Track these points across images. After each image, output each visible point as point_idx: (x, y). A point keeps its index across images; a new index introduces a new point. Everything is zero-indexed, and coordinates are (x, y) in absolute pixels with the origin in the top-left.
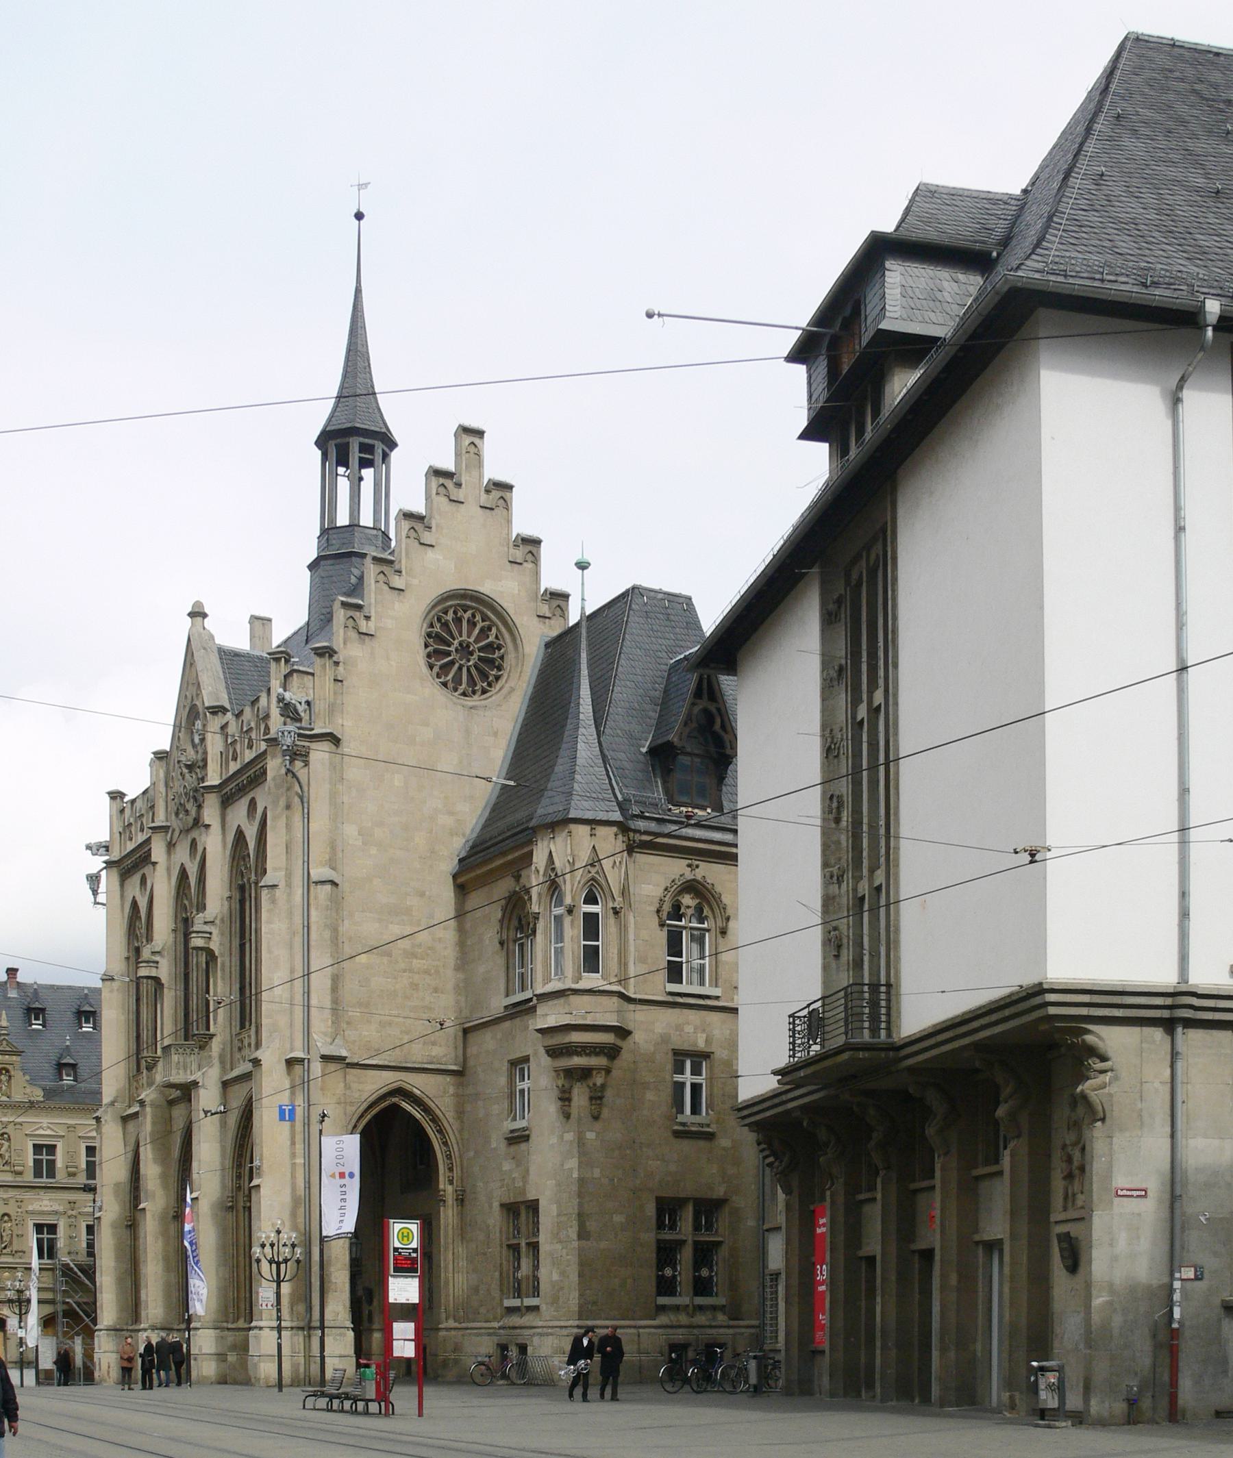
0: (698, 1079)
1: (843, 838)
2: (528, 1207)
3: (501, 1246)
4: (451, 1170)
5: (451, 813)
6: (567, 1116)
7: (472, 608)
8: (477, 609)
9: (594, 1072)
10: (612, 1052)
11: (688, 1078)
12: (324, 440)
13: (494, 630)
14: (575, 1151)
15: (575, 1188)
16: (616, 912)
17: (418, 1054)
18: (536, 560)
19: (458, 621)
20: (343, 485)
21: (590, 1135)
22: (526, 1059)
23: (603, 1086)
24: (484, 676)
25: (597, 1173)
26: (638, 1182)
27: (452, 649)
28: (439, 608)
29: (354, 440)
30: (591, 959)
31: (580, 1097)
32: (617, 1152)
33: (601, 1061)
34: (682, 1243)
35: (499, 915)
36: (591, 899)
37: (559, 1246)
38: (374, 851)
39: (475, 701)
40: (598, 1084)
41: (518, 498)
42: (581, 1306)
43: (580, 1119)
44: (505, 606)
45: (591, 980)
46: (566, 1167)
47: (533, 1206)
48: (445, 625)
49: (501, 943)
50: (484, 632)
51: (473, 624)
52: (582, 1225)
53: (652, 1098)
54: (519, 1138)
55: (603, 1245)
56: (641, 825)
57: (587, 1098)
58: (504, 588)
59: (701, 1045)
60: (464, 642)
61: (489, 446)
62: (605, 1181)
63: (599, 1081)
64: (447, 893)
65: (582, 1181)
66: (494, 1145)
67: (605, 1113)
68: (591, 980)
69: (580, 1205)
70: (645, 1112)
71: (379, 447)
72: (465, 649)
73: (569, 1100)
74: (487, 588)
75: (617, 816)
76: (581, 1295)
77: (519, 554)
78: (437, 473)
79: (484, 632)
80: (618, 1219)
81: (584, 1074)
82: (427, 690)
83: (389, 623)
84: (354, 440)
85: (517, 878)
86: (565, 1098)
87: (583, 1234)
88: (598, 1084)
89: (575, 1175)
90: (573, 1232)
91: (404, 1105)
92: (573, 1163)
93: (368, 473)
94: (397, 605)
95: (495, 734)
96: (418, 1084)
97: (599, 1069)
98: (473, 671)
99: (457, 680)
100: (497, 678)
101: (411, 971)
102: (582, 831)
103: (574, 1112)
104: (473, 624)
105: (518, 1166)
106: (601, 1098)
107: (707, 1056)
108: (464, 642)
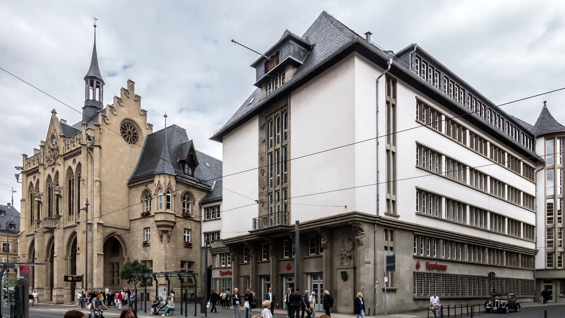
0: (189, 235)
1: (264, 179)
6: (162, 241)
10: (172, 227)
11: (186, 235)
12: (86, 78)
16: (174, 196)
17: (119, 225)
19: (128, 126)
20: (91, 91)
21: (167, 246)
22: (149, 228)
25: (168, 254)
29: (94, 80)
30: (168, 206)
31: (165, 237)
35: (141, 194)
36: (168, 192)
39: (132, 145)
45: (168, 211)
47: (151, 262)
48: (125, 126)
51: (131, 127)
56: (178, 177)
58: (139, 120)
59: (189, 228)
60: (129, 131)
63: (170, 233)
64: (126, 188)
65: (166, 256)
68: (168, 211)
71: (101, 84)
72: (129, 133)
74: (135, 119)
75: (175, 174)
77: (142, 113)
80: (173, 265)
81: (166, 232)
82: (121, 140)
84: (94, 80)
85: (146, 186)
86: (161, 237)
93: (98, 89)
99: (128, 139)
102: (167, 177)
104: (131, 127)
107: (190, 230)
108: (129, 131)
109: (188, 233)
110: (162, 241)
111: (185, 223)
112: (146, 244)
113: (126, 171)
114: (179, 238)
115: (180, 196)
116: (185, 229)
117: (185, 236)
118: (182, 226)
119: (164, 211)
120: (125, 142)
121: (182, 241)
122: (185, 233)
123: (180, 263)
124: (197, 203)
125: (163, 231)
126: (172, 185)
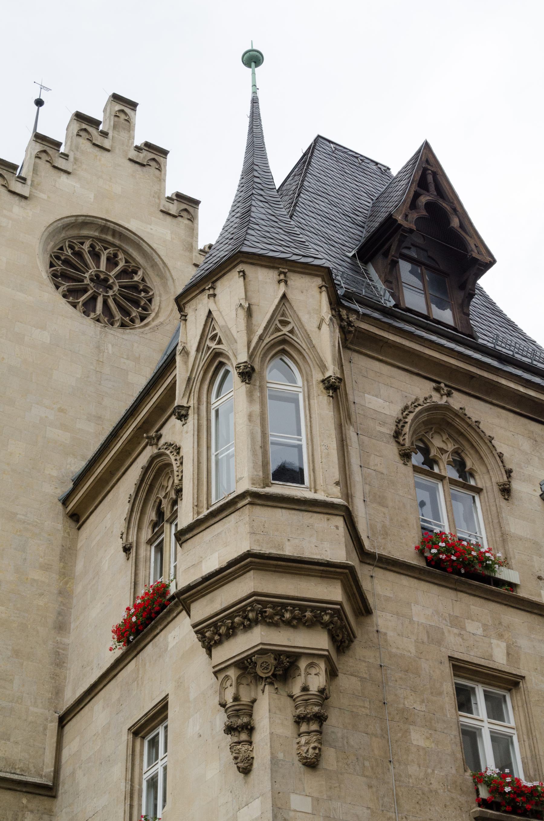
6: (246, 769)
8: (120, 248)
9: (303, 664)
10: (343, 640)
13: (140, 273)
18: (193, 219)
23: (323, 694)
24: (125, 312)
27: (87, 275)
28: (74, 232)
31: (271, 714)
33: (319, 641)
40: (314, 689)
41: (171, 163)
43: (274, 761)
44: (154, 246)
49: (127, 550)
50: (127, 273)
51: (112, 261)
53: (422, 743)
57: (290, 722)
61: (140, 118)
63: (317, 681)
67: (330, 758)
70: (413, 769)
73: (249, 729)
74: (133, 225)
77: (174, 208)
78: (79, 117)
86: (240, 725)
97: (314, 656)
100: (142, 319)
106: (320, 718)
109: (496, 711)
110: (246, 769)
111: (456, 622)
114: (418, 738)
115: (389, 430)
116: (459, 667)
117: (470, 736)
118: (434, 637)
120: (63, 305)
121: (449, 766)
122: (464, 702)
125: (245, 666)
126: (309, 322)
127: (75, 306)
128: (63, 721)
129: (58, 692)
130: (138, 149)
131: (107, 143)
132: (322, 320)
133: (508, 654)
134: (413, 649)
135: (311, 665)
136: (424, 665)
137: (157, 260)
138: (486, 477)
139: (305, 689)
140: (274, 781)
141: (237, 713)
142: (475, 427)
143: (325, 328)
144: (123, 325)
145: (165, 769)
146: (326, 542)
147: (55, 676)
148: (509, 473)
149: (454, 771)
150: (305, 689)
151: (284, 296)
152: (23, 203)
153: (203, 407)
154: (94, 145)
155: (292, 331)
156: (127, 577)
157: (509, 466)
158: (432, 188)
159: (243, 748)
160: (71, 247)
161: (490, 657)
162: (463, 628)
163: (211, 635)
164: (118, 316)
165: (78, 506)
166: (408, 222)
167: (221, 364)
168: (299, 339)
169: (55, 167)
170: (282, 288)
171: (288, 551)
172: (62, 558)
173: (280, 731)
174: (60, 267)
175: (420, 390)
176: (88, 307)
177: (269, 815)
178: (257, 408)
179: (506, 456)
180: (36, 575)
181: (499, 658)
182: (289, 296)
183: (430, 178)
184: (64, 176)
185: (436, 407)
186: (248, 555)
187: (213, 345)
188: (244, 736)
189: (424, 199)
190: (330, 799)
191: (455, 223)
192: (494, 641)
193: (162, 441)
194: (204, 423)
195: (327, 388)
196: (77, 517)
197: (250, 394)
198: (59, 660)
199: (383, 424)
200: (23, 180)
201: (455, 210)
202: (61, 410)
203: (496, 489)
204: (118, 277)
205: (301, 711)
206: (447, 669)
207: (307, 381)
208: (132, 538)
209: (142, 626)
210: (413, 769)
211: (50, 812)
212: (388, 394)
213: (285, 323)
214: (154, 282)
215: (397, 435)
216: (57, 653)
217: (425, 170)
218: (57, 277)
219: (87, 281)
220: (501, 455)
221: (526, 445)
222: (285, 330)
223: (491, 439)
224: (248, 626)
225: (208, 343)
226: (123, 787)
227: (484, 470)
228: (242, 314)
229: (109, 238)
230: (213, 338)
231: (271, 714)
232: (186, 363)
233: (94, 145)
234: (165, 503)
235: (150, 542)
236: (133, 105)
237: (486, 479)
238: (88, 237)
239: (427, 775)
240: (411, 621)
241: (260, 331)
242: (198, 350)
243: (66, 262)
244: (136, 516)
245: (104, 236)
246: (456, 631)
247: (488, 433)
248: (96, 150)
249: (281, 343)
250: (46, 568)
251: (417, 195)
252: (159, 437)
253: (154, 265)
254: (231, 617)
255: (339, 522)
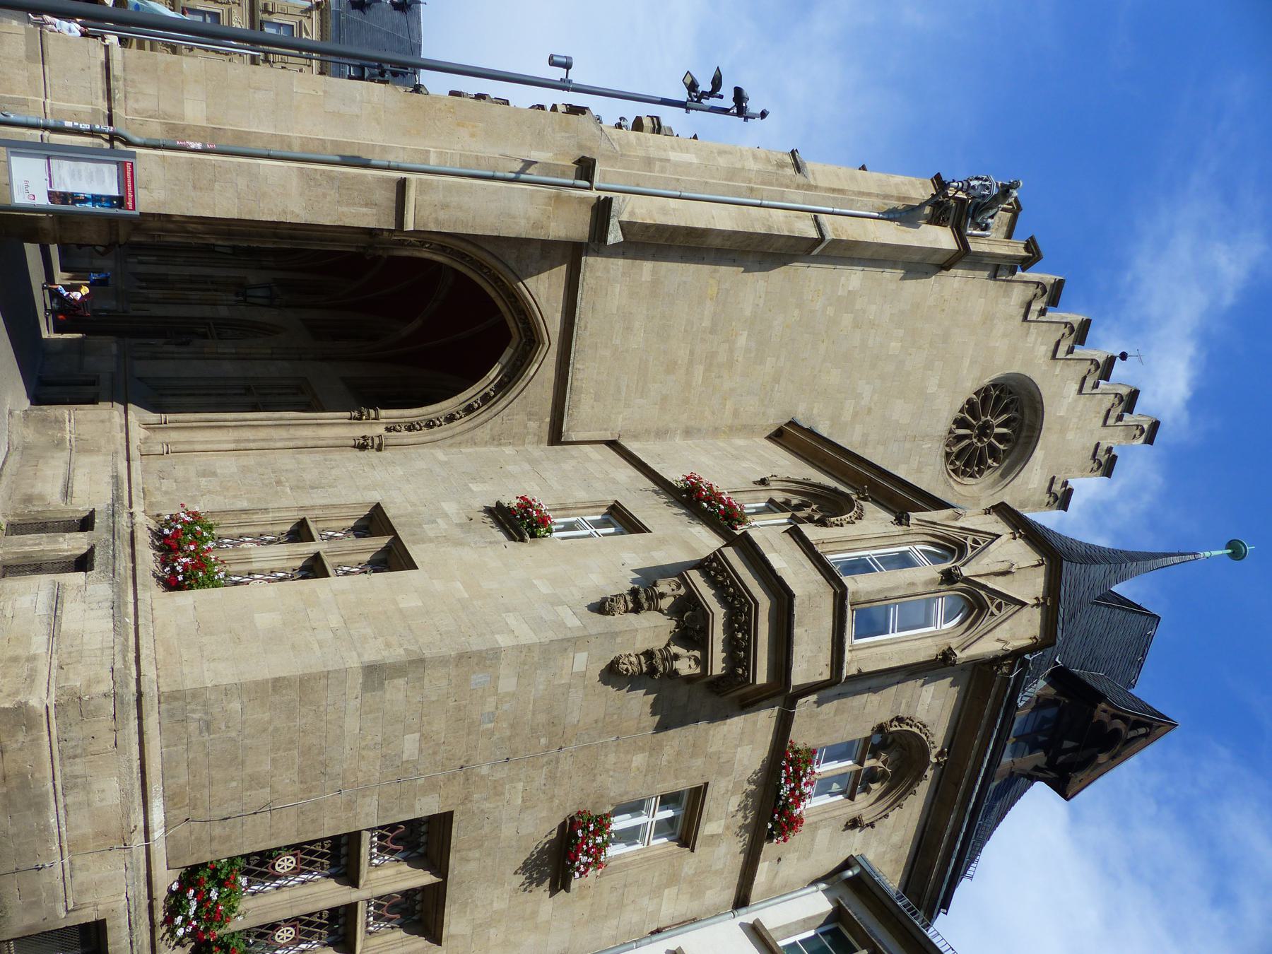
2: (387, 550)
3: (302, 508)
4: (410, 428)
5: (855, 415)
7: (1018, 438)
9: (697, 653)
14: (551, 635)
15: (476, 644)
24: (959, 456)
25: (507, 683)
26: (485, 770)
31: (652, 630)
32: (542, 718)
33: (718, 667)
34: (348, 874)
37: (335, 621)
38: (830, 311)
40: (677, 665)
42: (195, 694)
43: (613, 635)
44: (1022, 474)
46: (511, 620)
49: (763, 482)
50: (994, 452)
51: (1001, 438)
52: (398, 670)
54: (518, 522)
55: (352, 724)
62: (490, 706)
65: (487, 659)
66: (474, 487)
69: (443, 661)
72: (984, 430)
73: (637, 609)
74: (1039, 453)
76: (226, 691)
77: (1057, 488)
78: (1134, 395)
79: (994, 452)
80: (410, 745)
83: (1031, 339)
87: (375, 674)
88: (677, 665)
89: (503, 641)
90: (374, 653)
91: (509, 352)
92: (527, 635)
94: (1043, 348)
95: (919, 470)
96: (543, 370)
97: (703, 662)
98: (966, 442)
101: (691, 363)
103: (623, 621)
105: (461, 526)
109: (663, 828)
112: (518, 522)
113: (849, 407)
114: (639, 760)
118: (724, 768)
119: (854, 584)
120: (961, 401)
122: (667, 800)
123: (427, 806)
124: (854, 844)
127: (961, 411)
128: (613, 445)
129: (636, 437)
130: (1109, 450)
131: (1111, 421)
132: (1006, 643)
133: (712, 836)
134: (713, 749)
135: (697, 660)
136: (699, 762)
137: (1009, 478)
138: (865, 804)
139: (676, 657)
140: (598, 636)
141: (649, 598)
142: (909, 790)
143: (999, 646)
144: (948, 455)
145: (590, 536)
146: (809, 663)
147: (648, 432)
148: (872, 825)
149: (612, 794)
150: (676, 657)
151: (1023, 604)
152: (1050, 354)
153: (910, 538)
154: (1109, 411)
155: (992, 614)
156: (738, 484)
157: (876, 824)
158: (1132, 734)
159: (622, 606)
160: (1012, 401)
161: (709, 820)
162: (733, 794)
163: (711, 567)
164: (955, 449)
165: (789, 436)
166: (1101, 712)
167: (952, 552)
168: (986, 622)
169: (1084, 379)
170: (1031, 602)
171: (798, 631)
172: (745, 427)
173: (639, 637)
174: (994, 393)
175: (938, 737)
176: (960, 423)
177: (569, 635)
178: (920, 590)
179: (886, 821)
180: (729, 405)
181: (708, 828)
182: (1026, 609)
183: (1142, 731)
184: (1077, 387)
185: (926, 752)
186: (790, 596)
187: (969, 542)
188: (631, 606)
189: (1119, 724)
190: (585, 687)
191: (1103, 758)
192: (723, 822)
193: (863, 503)
194: (897, 540)
195: (944, 653)
196: (778, 436)
197: (931, 582)
198: (662, 434)
199: (909, 706)
200: (1071, 351)
201: (1113, 758)
202: (870, 410)
203: (855, 814)
204: (990, 445)
205: (658, 655)
206: (698, 782)
207: (948, 633)
208: (774, 485)
209: (693, 499)
210: (612, 758)
211: (539, 442)
212: (932, 707)
213: (999, 607)
214: (988, 477)
215: (900, 720)
216: (666, 432)
217: (1149, 725)
218: (984, 393)
219: (983, 419)
220: (886, 816)
221: (896, 839)
222: (993, 609)
223: (900, 806)
224: (723, 599)
225: (970, 538)
226: (570, 502)
227: (872, 800)
228: (1004, 567)
229: (1024, 434)
230: (975, 541)
231: (652, 630)
232: (948, 518)
233: (1109, 411)
234: (809, 511)
235: (771, 501)
236: (1150, 440)
237: (863, 804)
238: (1022, 414)
239: (607, 771)
240: (737, 746)
241: (990, 585)
242: (962, 528)
243: (998, 398)
244: (793, 486)
245: (1025, 429)
246: (730, 787)
247: (905, 803)
248: (1104, 413)
249: (976, 603)
250: (736, 414)
251: (1125, 720)
252: (865, 499)
253: (1003, 476)
254: (733, 584)
255: (826, 676)
